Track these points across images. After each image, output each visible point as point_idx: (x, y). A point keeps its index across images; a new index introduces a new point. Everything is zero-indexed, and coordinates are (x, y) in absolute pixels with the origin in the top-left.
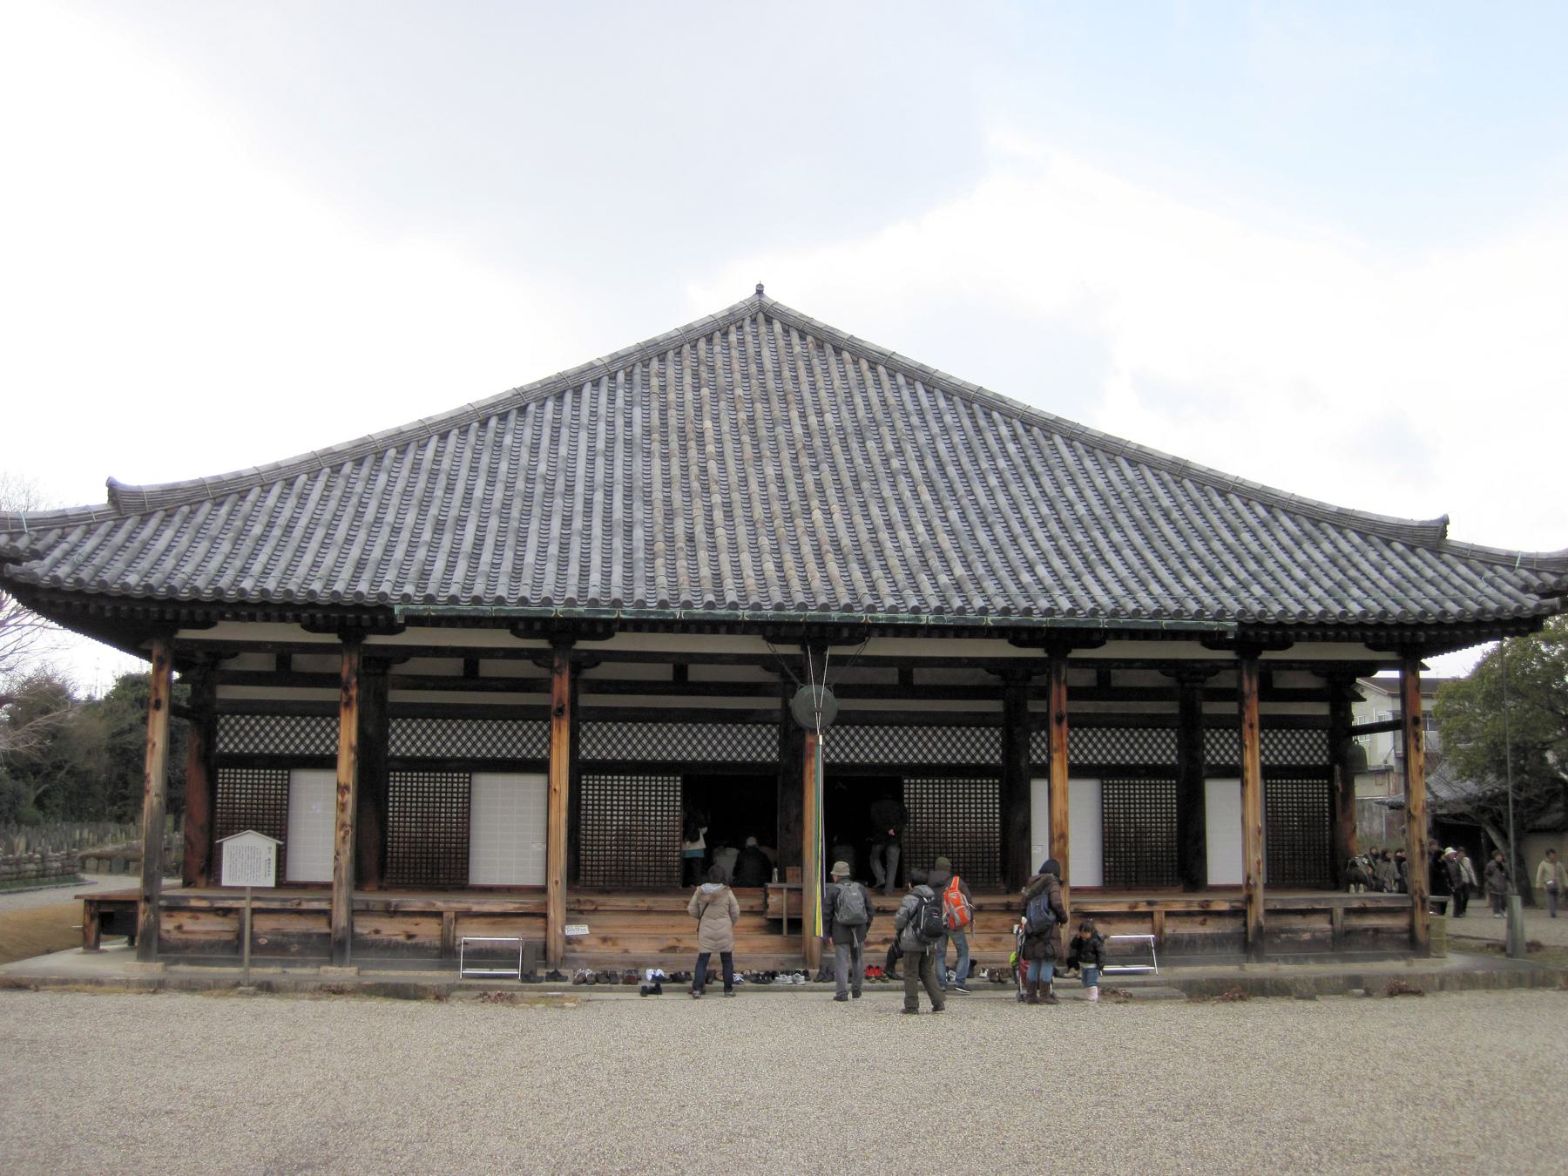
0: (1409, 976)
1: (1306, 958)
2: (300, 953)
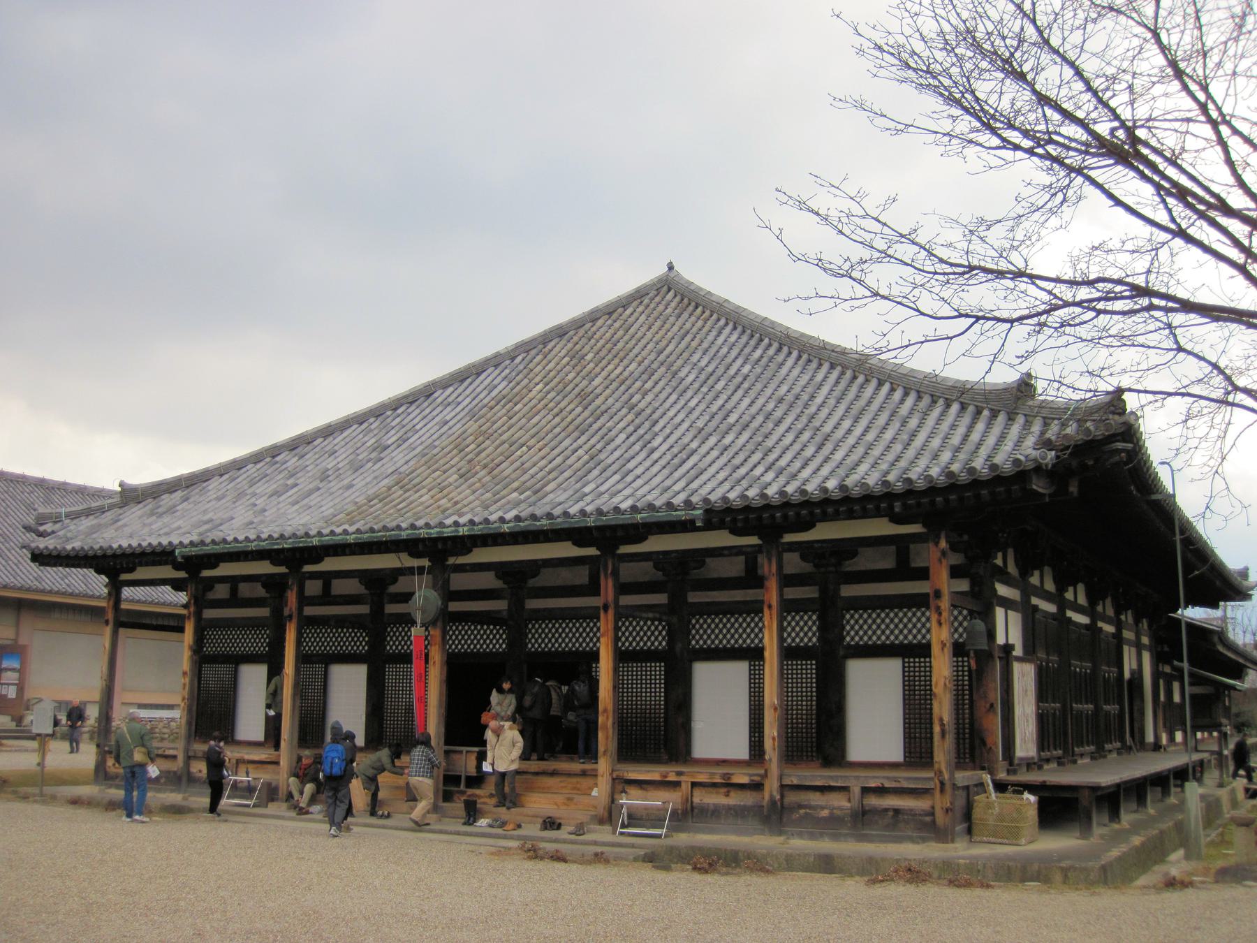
0: (883, 859)
1: (822, 835)
2: (165, 784)
